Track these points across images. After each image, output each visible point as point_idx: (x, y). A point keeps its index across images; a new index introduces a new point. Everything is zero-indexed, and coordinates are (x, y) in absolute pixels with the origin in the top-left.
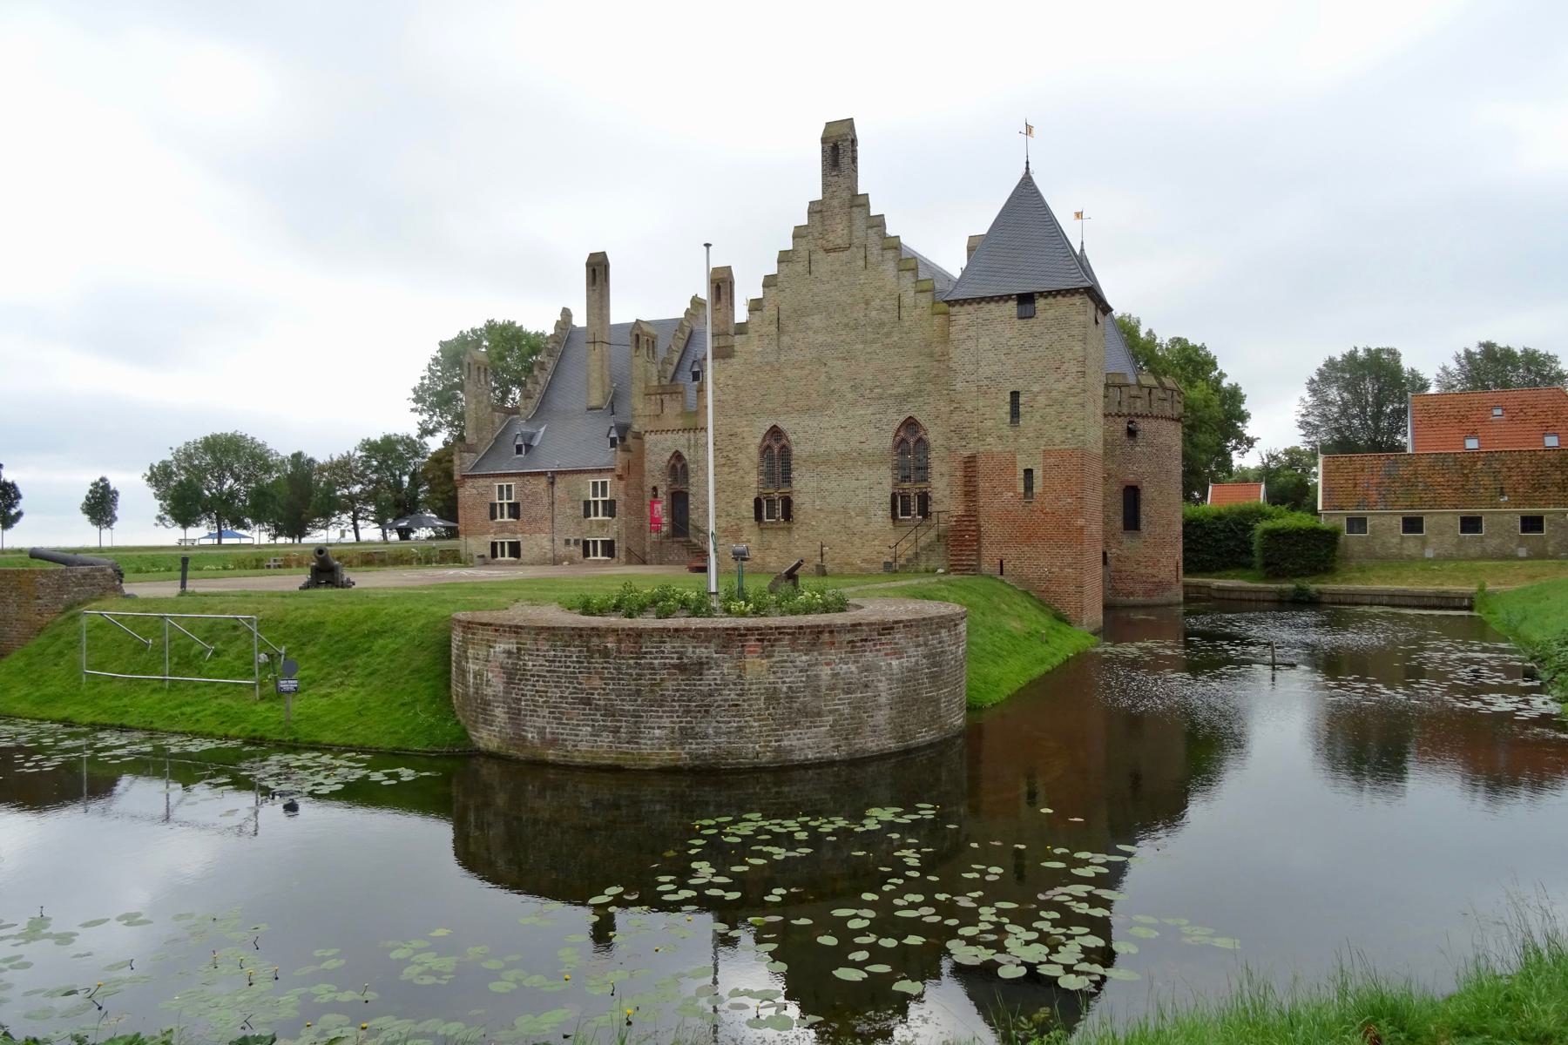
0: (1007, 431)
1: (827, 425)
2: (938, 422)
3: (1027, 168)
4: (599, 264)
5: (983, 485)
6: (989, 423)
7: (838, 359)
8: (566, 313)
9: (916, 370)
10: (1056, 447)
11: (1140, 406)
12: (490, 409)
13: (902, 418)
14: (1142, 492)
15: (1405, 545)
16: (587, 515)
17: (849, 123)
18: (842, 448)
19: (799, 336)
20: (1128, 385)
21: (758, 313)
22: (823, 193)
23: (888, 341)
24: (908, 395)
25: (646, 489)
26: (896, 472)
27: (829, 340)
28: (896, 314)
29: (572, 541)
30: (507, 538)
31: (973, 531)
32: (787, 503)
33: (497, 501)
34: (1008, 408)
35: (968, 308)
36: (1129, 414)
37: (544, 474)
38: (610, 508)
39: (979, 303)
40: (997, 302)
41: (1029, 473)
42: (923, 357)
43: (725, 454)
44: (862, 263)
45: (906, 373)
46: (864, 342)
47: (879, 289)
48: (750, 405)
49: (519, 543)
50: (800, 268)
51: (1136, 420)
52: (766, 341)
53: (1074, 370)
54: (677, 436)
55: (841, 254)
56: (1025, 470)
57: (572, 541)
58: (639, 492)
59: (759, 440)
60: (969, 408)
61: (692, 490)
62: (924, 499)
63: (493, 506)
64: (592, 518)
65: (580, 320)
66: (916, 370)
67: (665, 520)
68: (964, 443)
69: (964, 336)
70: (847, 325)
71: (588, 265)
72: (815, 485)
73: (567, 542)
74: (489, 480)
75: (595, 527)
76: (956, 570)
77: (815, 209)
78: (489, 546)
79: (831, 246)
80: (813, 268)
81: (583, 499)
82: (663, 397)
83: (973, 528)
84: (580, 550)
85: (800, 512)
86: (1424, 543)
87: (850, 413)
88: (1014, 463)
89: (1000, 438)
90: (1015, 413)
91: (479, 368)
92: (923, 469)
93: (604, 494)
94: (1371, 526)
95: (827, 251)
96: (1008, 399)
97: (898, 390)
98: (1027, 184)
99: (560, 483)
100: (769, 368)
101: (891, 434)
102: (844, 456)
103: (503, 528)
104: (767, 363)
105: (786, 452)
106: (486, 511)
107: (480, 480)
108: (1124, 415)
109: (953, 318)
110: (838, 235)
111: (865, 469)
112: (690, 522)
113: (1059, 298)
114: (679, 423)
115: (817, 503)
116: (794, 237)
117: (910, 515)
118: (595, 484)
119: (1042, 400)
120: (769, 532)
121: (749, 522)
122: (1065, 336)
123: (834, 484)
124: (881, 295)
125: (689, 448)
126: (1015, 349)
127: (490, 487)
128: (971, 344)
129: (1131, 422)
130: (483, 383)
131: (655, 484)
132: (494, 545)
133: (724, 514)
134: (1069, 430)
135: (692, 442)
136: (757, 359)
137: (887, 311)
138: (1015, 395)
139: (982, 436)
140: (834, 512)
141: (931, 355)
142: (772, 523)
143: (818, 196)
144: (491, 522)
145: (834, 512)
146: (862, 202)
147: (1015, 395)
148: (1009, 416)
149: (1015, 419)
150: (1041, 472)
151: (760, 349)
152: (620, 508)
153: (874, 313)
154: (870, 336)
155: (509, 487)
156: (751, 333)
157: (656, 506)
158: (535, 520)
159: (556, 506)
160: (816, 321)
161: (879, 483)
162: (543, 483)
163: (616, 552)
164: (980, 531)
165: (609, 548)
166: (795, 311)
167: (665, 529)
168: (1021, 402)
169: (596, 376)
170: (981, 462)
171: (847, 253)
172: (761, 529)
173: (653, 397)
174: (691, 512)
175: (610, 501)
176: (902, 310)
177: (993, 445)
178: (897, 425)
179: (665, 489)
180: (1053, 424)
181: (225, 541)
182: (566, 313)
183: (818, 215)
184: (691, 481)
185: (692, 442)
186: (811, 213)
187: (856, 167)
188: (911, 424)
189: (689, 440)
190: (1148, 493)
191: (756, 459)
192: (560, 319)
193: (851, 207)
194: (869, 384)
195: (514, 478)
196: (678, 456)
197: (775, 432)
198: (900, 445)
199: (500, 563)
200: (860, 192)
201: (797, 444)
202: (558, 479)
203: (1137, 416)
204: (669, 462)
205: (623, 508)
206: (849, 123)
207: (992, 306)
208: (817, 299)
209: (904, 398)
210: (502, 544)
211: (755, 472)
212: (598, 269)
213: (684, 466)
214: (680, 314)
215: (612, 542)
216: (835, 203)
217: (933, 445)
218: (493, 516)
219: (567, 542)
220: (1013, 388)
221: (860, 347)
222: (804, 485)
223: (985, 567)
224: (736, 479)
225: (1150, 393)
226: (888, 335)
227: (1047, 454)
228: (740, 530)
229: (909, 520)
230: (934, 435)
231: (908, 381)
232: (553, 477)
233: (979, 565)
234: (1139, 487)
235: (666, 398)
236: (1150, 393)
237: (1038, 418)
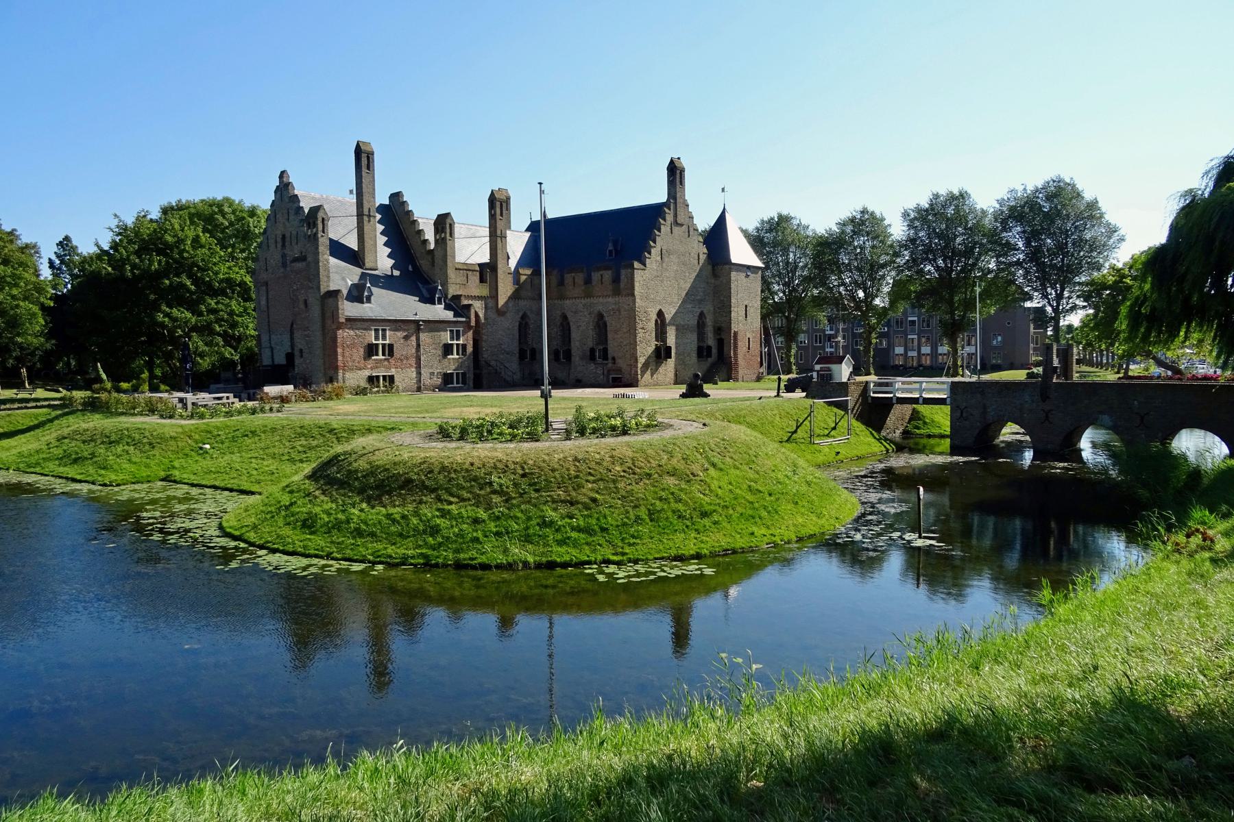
0: (745, 322)
13: (699, 310)
33: (374, 342)
61: (485, 337)
97: (699, 298)
107: (359, 323)
138: (746, 306)
141: (707, 283)
147: (746, 306)
175: (389, 345)
178: (698, 314)
195: (388, 324)
209: (700, 301)
210: (378, 377)
215: (464, 374)
220: (746, 303)
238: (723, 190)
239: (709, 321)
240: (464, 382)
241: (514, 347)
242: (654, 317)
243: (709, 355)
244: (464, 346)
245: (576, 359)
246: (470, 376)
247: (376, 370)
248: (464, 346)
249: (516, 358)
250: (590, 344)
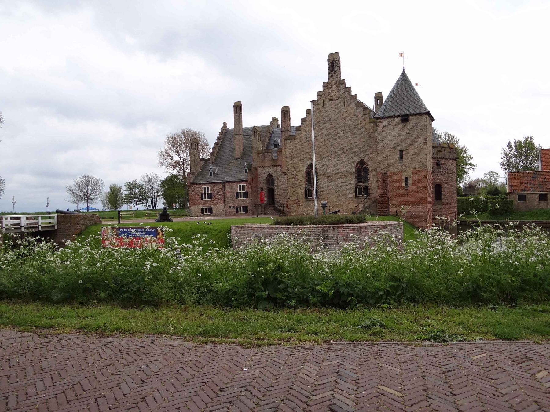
0: (398, 164)
1: (331, 163)
2: (372, 161)
3: (404, 69)
4: (238, 106)
5: (390, 183)
6: (392, 161)
7: (335, 139)
8: (225, 124)
9: (363, 143)
10: (417, 170)
11: (441, 155)
12: (199, 159)
13: (358, 160)
14: (442, 186)
15: (540, 205)
16: (237, 197)
17: (337, 54)
18: (336, 171)
19: (319, 131)
20: (436, 147)
21: (304, 123)
22: (328, 79)
23: (353, 132)
24: (361, 151)
25: (258, 188)
26: (356, 179)
27: (331, 132)
28: (356, 122)
29: (232, 207)
30: (207, 207)
31: (386, 200)
34: (398, 156)
35: (384, 120)
36: (437, 158)
37: (222, 182)
38: (246, 195)
39: (387, 118)
40: (394, 118)
41: (406, 179)
42: (366, 138)
43: (293, 174)
44: (343, 104)
45: (360, 144)
46: (344, 133)
47: (350, 113)
48: (302, 156)
49: (212, 208)
50: (320, 107)
51: (440, 160)
52: (308, 133)
53: (423, 142)
54: (270, 168)
55: (335, 101)
56: (405, 178)
57: (232, 207)
58: (256, 189)
59: (305, 169)
60: (384, 156)
61: (276, 188)
62: (367, 190)
63: (202, 195)
64: (239, 198)
65: (231, 126)
66: (363, 143)
67: (265, 199)
68: (382, 169)
69: (382, 130)
70: (337, 127)
71: (234, 106)
72: (326, 184)
73: (230, 207)
74: (201, 185)
75: (240, 202)
76: (379, 214)
77: (325, 85)
78: (201, 209)
79: (331, 98)
80: (325, 106)
81: (236, 192)
82: (264, 154)
83: (386, 199)
84: (235, 210)
85: (321, 195)
86: (548, 204)
87: (339, 159)
88: (401, 175)
89: (396, 166)
90: (401, 157)
91: (195, 144)
92: (366, 178)
93: (243, 190)
94: (527, 198)
95: (330, 100)
96: (399, 153)
97: (356, 150)
98: (404, 74)
99: (227, 186)
100: (309, 143)
101: (355, 166)
102: (337, 174)
104: (308, 141)
106: (200, 196)
107: (197, 185)
108: (435, 158)
109: (378, 124)
110: (334, 93)
111: (345, 179)
112: (275, 199)
113: (417, 116)
114: (271, 163)
115: (327, 191)
116: (318, 96)
117: (362, 195)
118: (240, 186)
119: (411, 153)
120: (310, 202)
121: (302, 199)
122: (420, 130)
123: (333, 184)
124: (350, 116)
125: (274, 172)
126: (401, 134)
127: (201, 188)
128: (385, 133)
129: (439, 161)
130: (197, 150)
131: (262, 186)
132: (202, 209)
133: (293, 196)
134: (421, 163)
135: (275, 170)
136: (305, 140)
137: (352, 122)
138: (401, 151)
139: (389, 166)
140: (333, 194)
141: (369, 137)
142: (311, 198)
143: (326, 80)
144: (201, 201)
145: (333, 194)
146: (343, 82)
147: (401, 151)
148: (399, 159)
149: (401, 160)
150: (411, 179)
151: (306, 136)
152: (250, 195)
153: (348, 122)
154: (346, 131)
155: (208, 188)
156: (302, 130)
157: (262, 194)
158: (218, 200)
159: (225, 195)
160: (326, 126)
161: (351, 183)
162: (221, 186)
163: (248, 211)
164: (388, 200)
165: (246, 209)
166: (319, 122)
167: (266, 202)
168: (403, 153)
169: (238, 146)
170: (389, 175)
171: (338, 101)
172: (307, 201)
173: (261, 154)
174: (275, 196)
176: (358, 121)
178: (356, 162)
179: (265, 188)
180: (415, 161)
181: (89, 211)
182: (225, 124)
183: (327, 87)
184: (275, 184)
185: (275, 170)
186: (324, 86)
187: (340, 70)
188: (362, 162)
189: (274, 170)
190: (444, 187)
191: (305, 176)
192: (223, 126)
193: (339, 84)
194: (346, 148)
196: (270, 175)
198: (358, 170)
199: (205, 216)
200: (342, 78)
201: (320, 170)
202: (226, 184)
203: (440, 158)
204: (267, 178)
205: (251, 195)
206: (337, 54)
207: (392, 119)
208: (326, 118)
209: (359, 153)
210: (206, 208)
211: (304, 180)
212: (238, 108)
213: (273, 179)
214: (268, 123)
216: (333, 83)
217: (370, 169)
218: (202, 198)
219: (230, 207)
220: (400, 148)
221: (342, 134)
223: (391, 213)
224: (297, 183)
225: (445, 150)
226: (353, 130)
227: (413, 172)
228: (299, 201)
229: (362, 197)
230: (371, 166)
231: (360, 147)
232: (224, 184)
233: (388, 212)
234: (441, 184)
235: (266, 154)
236: (445, 150)
237: (410, 159)
238: (402, 55)
242: (303, 169)
247: (205, 205)
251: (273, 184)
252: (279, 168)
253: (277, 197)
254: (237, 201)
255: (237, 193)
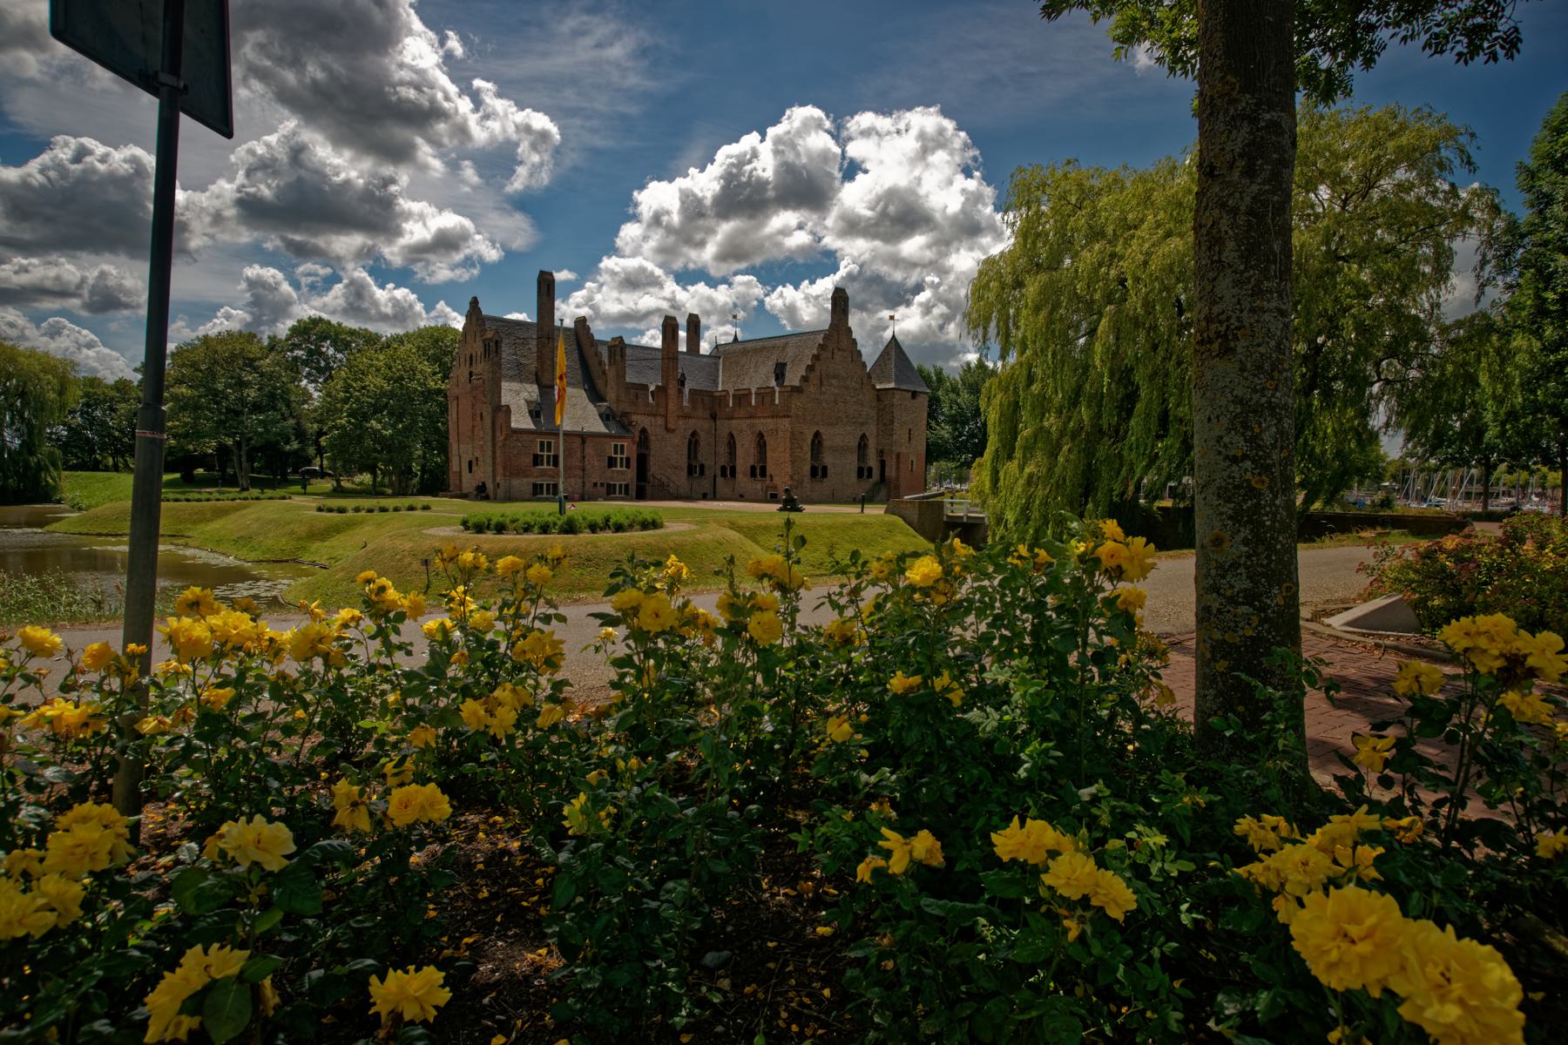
32: (825, 469)
84: (604, 490)
103: (543, 473)
105: (820, 443)
121: (807, 479)
132: (535, 486)
146: (850, 331)
160: (834, 382)
161: (852, 461)
162: (578, 441)
177: (903, 450)
188: (863, 437)
196: (644, 431)
197: (817, 434)
202: (589, 443)
222: (828, 459)
239: (872, 443)
240: (627, 492)
241: (684, 462)
243: (870, 476)
244: (628, 459)
245: (739, 476)
246: (633, 489)
248: (628, 459)
249: (684, 474)
250: (752, 462)
251: (648, 448)
252: (660, 421)
253: (654, 468)
254: (609, 472)
255: (610, 459)
